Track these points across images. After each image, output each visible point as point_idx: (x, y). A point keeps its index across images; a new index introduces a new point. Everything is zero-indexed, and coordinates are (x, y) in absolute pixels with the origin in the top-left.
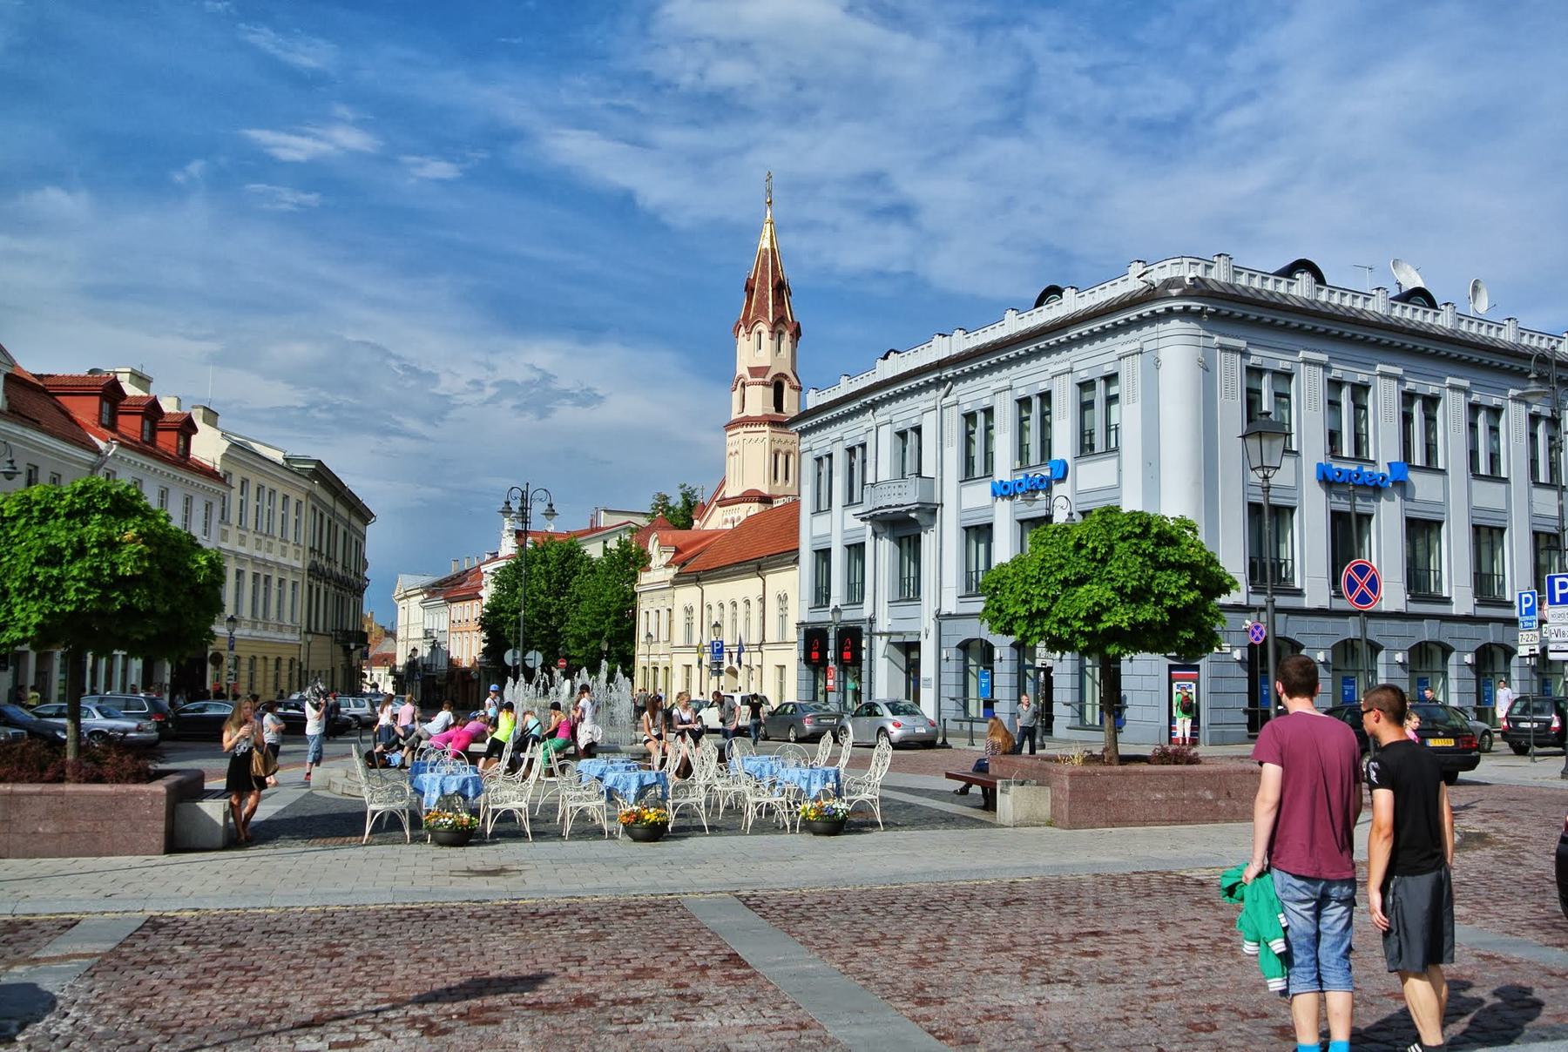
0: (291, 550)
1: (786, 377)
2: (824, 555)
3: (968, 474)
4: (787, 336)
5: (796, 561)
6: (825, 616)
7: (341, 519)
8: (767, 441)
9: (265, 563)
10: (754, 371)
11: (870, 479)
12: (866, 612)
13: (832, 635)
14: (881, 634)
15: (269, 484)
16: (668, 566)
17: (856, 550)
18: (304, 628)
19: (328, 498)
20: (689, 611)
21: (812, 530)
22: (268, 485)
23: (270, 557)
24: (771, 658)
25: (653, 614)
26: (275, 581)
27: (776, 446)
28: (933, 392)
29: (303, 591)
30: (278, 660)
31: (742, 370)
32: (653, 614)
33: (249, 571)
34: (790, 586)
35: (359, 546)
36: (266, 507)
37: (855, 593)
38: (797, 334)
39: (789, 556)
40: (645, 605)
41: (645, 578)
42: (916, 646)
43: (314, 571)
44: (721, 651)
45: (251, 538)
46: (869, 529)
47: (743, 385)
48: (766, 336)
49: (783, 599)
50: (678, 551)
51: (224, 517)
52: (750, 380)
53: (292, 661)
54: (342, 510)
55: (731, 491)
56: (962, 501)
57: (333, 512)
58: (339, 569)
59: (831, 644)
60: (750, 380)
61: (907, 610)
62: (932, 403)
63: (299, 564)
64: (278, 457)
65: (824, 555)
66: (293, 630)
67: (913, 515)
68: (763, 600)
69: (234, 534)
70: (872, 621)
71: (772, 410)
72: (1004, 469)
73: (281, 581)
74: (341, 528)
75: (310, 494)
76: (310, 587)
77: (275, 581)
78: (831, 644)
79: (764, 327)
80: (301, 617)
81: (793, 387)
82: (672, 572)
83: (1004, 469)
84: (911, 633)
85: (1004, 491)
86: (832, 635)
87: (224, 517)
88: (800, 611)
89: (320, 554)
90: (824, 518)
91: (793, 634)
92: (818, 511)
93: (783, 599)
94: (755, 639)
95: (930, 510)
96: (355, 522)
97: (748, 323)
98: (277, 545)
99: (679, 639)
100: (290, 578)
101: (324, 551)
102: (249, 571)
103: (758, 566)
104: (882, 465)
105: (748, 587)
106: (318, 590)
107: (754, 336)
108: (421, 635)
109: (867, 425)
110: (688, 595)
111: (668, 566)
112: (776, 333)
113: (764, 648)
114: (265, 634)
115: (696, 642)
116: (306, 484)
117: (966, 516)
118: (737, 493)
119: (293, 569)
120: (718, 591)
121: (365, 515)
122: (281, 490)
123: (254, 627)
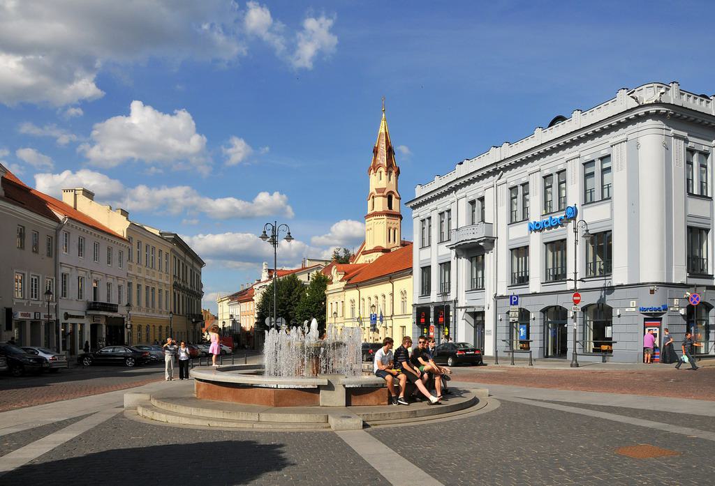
0: (164, 276)
1: (393, 193)
2: (426, 270)
4: (393, 174)
5: (411, 273)
6: (425, 301)
7: (189, 264)
8: (385, 223)
10: (378, 190)
11: (453, 226)
12: (452, 297)
13: (432, 310)
14: (461, 308)
16: (341, 281)
17: (446, 266)
19: (182, 254)
20: (353, 302)
21: (419, 257)
24: (397, 323)
25: (334, 304)
27: (389, 225)
29: (171, 295)
30: (160, 327)
31: (372, 189)
32: (334, 304)
34: (409, 287)
35: (199, 277)
36: (151, 255)
37: (445, 291)
38: (398, 173)
39: (408, 271)
40: (330, 299)
41: (330, 287)
42: (483, 313)
43: (175, 285)
44: (375, 319)
45: (144, 269)
46: (453, 252)
47: (373, 197)
48: (384, 174)
49: (404, 293)
50: (346, 274)
51: (130, 259)
52: (376, 194)
53: (167, 328)
54: (188, 259)
55: (368, 247)
56: (508, 235)
59: (432, 314)
60: (376, 194)
61: (477, 295)
62: (492, 183)
64: (157, 233)
65: (426, 270)
67: (481, 244)
68: (392, 294)
70: (456, 301)
71: (387, 208)
72: (536, 214)
73: (160, 291)
75: (172, 250)
76: (175, 294)
77: (157, 291)
78: (432, 314)
79: (382, 169)
80: (171, 307)
81: (397, 198)
83: (536, 214)
84: (479, 307)
85: (538, 228)
86: (432, 310)
87: (130, 259)
88: (414, 297)
89: (179, 278)
90: (427, 251)
91: (410, 310)
92: (423, 247)
93: (404, 293)
94: (388, 313)
95: (490, 242)
96: (196, 265)
97: (375, 167)
99: (348, 315)
101: (181, 277)
103: (390, 278)
104: (461, 217)
105: (385, 288)
106: (179, 295)
107: (378, 174)
108: (228, 317)
109: (451, 200)
110: (353, 294)
111: (341, 281)
112: (389, 172)
113: (393, 318)
114: (153, 315)
115: (357, 316)
116: (170, 245)
117: (511, 243)
118: (372, 248)
119: (165, 285)
120: (367, 292)
121: (201, 264)
123: (148, 311)
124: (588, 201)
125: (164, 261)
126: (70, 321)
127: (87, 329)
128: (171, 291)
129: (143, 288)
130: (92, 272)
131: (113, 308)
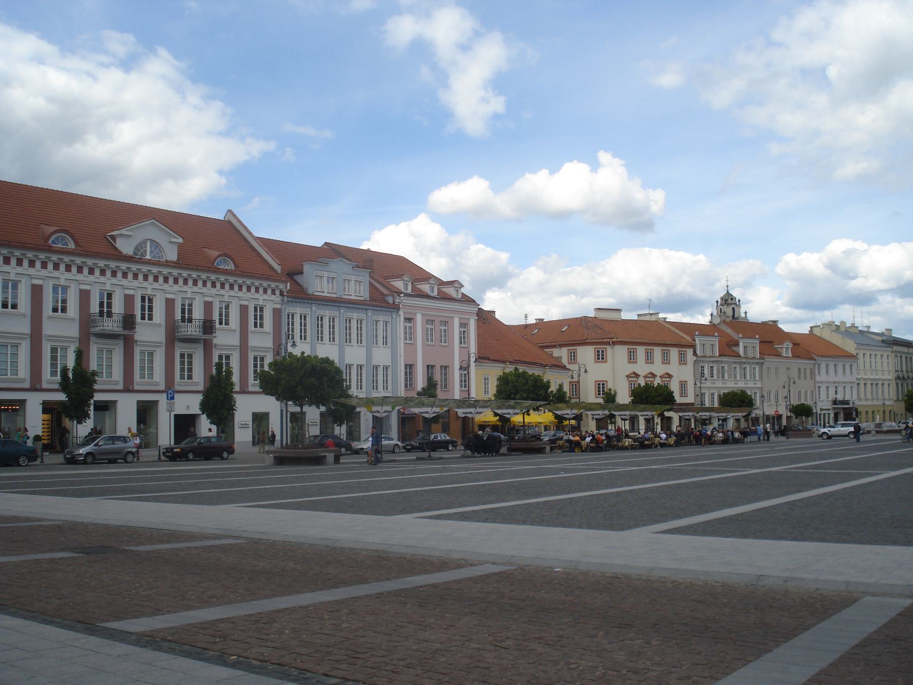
0: (886, 373)
9: (875, 380)
18: (895, 399)
19: (905, 349)
22: (873, 353)
23: (877, 377)
26: (880, 385)
29: (895, 385)
43: (898, 378)
63: (890, 377)
66: (890, 400)
75: (892, 352)
77: (880, 385)
89: (902, 371)
100: (886, 383)
102: (869, 383)
122: (879, 354)
126: (823, 412)
127: (832, 415)
129: (869, 386)
130: (834, 383)
131: (847, 402)
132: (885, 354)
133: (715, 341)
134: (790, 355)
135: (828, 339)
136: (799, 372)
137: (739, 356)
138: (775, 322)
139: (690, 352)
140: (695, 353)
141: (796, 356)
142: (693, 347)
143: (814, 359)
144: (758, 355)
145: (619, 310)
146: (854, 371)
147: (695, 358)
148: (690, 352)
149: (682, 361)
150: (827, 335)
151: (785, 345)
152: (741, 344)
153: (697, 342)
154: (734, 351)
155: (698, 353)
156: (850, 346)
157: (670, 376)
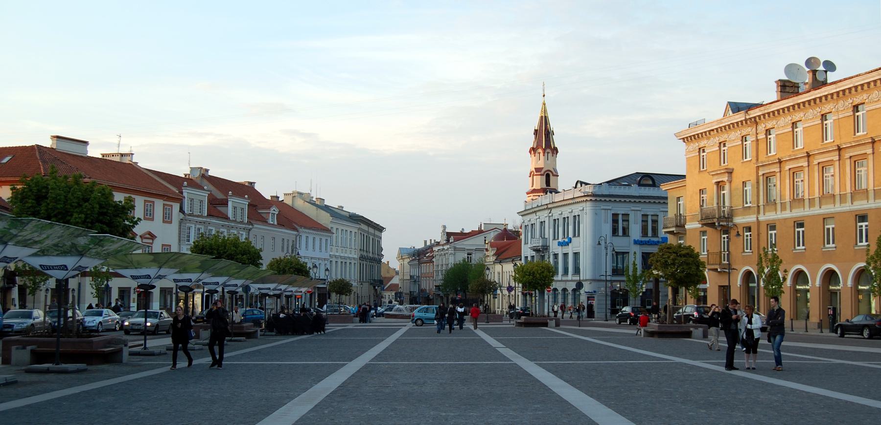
0: (353, 251)
3: (554, 239)
7: (371, 234)
9: (345, 258)
15: (345, 228)
22: (345, 228)
28: (547, 212)
29: (357, 266)
33: (339, 261)
35: (379, 242)
43: (362, 258)
48: (542, 154)
50: (498, 250)
54: (371, 230)
57: (368, 232)
58: (371, 255)
63: (356, 256)
69: (334, 248)
71: (545, 186)
74: (371, 237)
75: (359, 229)
81: (554, 175)
82: (495, 258)
96: (377, 233)
98: (348, 250)
102: (339, 261)
107: (537, 155)
122: (349, 230)
124: (574, 236)
125: (353, 238)
128: (357, 262)
130: (312, 258)
132: (354, 230)
133: (204, 196)
134: (276, 223)
135: (300, 210)
136: (283, 244)
137: (226, 218)
138: (251, 183)
139: (176, 207)
140: (181, 210)
141: (281, 224)
142: (180, 200)
143: (295, 229)
144: (246, 220)
145: (85, 143)
146: (329, 249)
147: (182, 216)
148: (176, 207)
149: (167, 219)
150: (300, 205)
151: (272, 211)
152: (230, 204)
153: (185, 194)
154: (220, 212)
155: (186, 209)
156: (324, 219)
157: (152, 236)
